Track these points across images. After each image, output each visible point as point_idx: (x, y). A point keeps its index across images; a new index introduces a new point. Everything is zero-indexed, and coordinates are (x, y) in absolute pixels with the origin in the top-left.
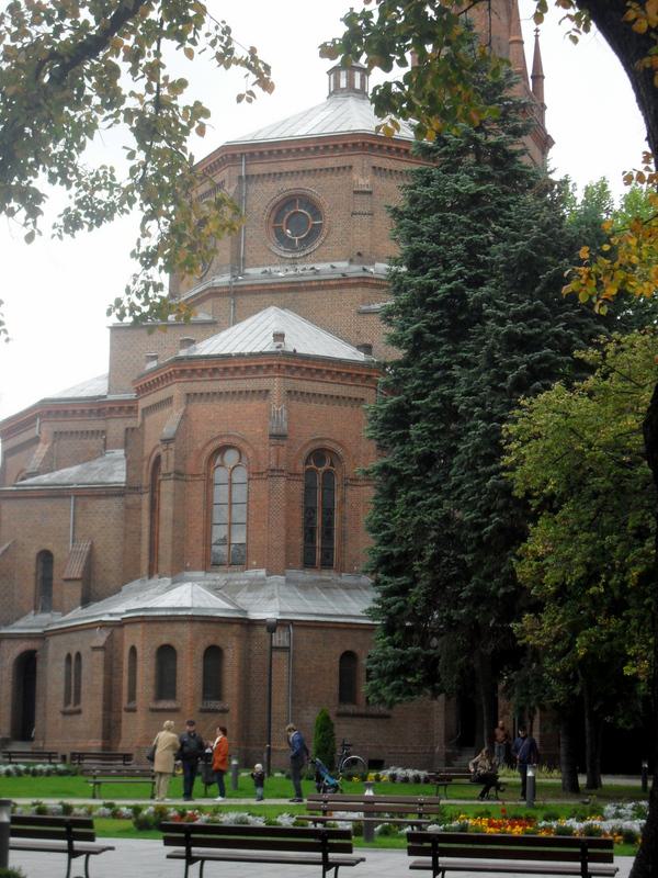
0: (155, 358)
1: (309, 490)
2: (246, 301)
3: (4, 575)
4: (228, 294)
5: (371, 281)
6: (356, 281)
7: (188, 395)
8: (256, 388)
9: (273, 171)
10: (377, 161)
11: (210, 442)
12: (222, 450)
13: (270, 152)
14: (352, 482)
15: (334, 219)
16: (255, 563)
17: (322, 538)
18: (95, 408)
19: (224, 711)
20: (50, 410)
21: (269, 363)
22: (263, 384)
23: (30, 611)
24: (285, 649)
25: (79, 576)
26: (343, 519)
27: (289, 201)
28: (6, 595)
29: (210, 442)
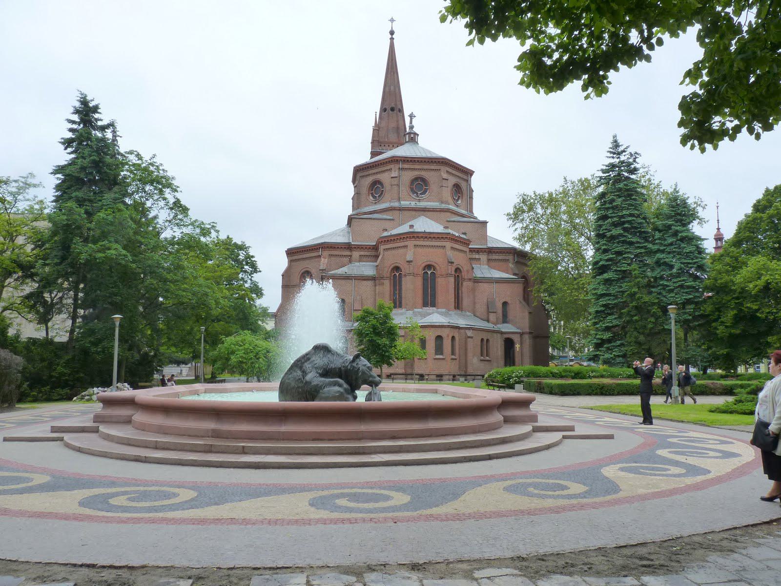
0: (386, 230)
2: (406, 213)
4: (400, 210)
8: (441, 245)
13: (411, 161)
15: (433, 187)
18: (348, 247)
19: (456, 359)
24: (472, 337)
27: (416, 179)
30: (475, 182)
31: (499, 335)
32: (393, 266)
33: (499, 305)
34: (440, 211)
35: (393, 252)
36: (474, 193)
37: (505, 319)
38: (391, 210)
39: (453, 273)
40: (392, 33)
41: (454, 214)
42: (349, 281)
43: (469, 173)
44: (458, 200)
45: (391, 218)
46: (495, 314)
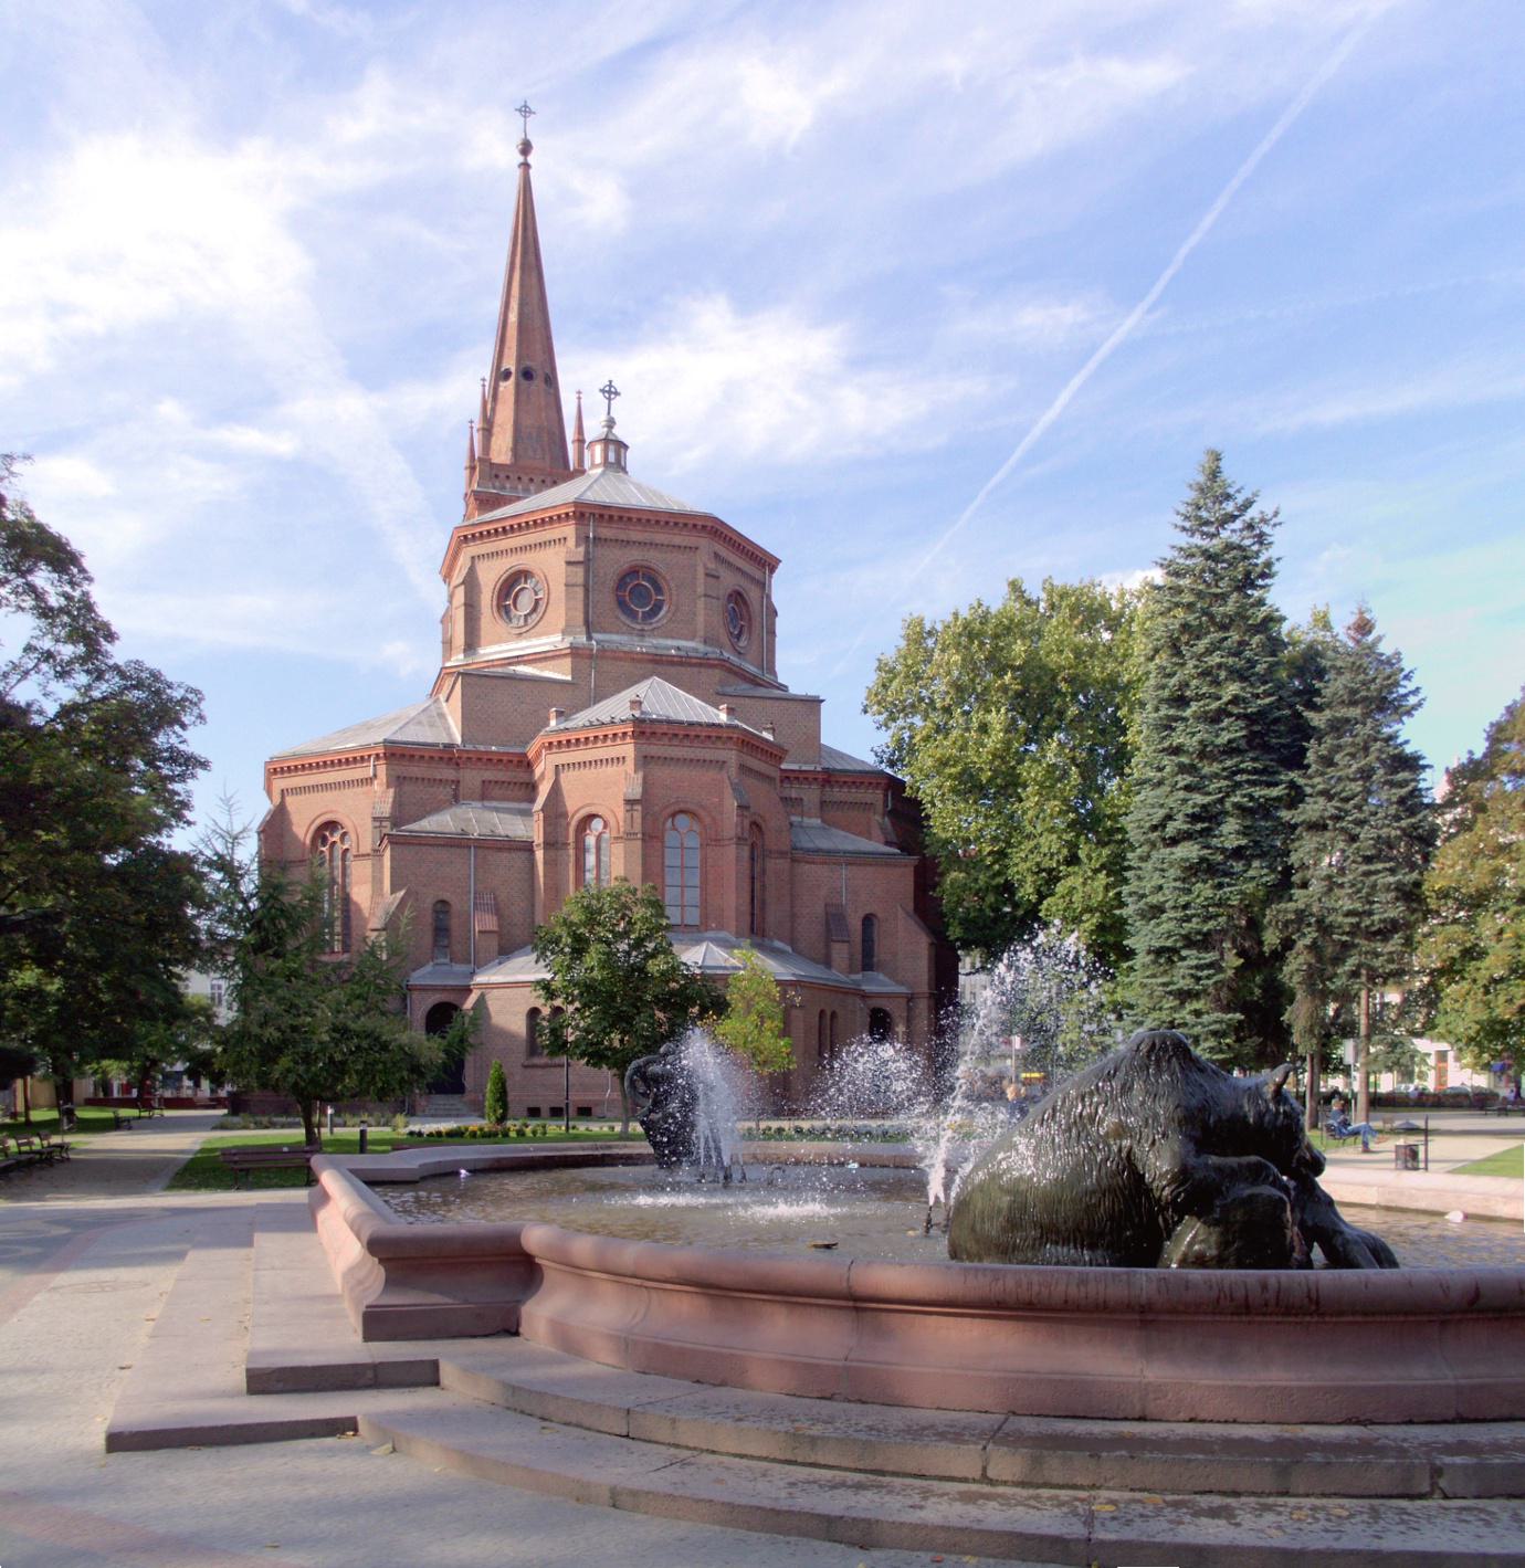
12: (674, 815)
18: (446, 755)
20: (396, 753)
25: (496, 929)
26: (763, 887)
27: (633, 572)
30: (781, 589)
31: (859, 1003)
33: (855, 924)
34: (701, 665)
35: (588, 774)
36: (777, 620)
37: (868, 962)
38: (565, 655)
39: (746, 835)
40: (526, 148)
41: (736, 674)
42: (458, 851)
43: (766, 563)
44: (738, 637)
45: (569, 678)
46: (845, 946)
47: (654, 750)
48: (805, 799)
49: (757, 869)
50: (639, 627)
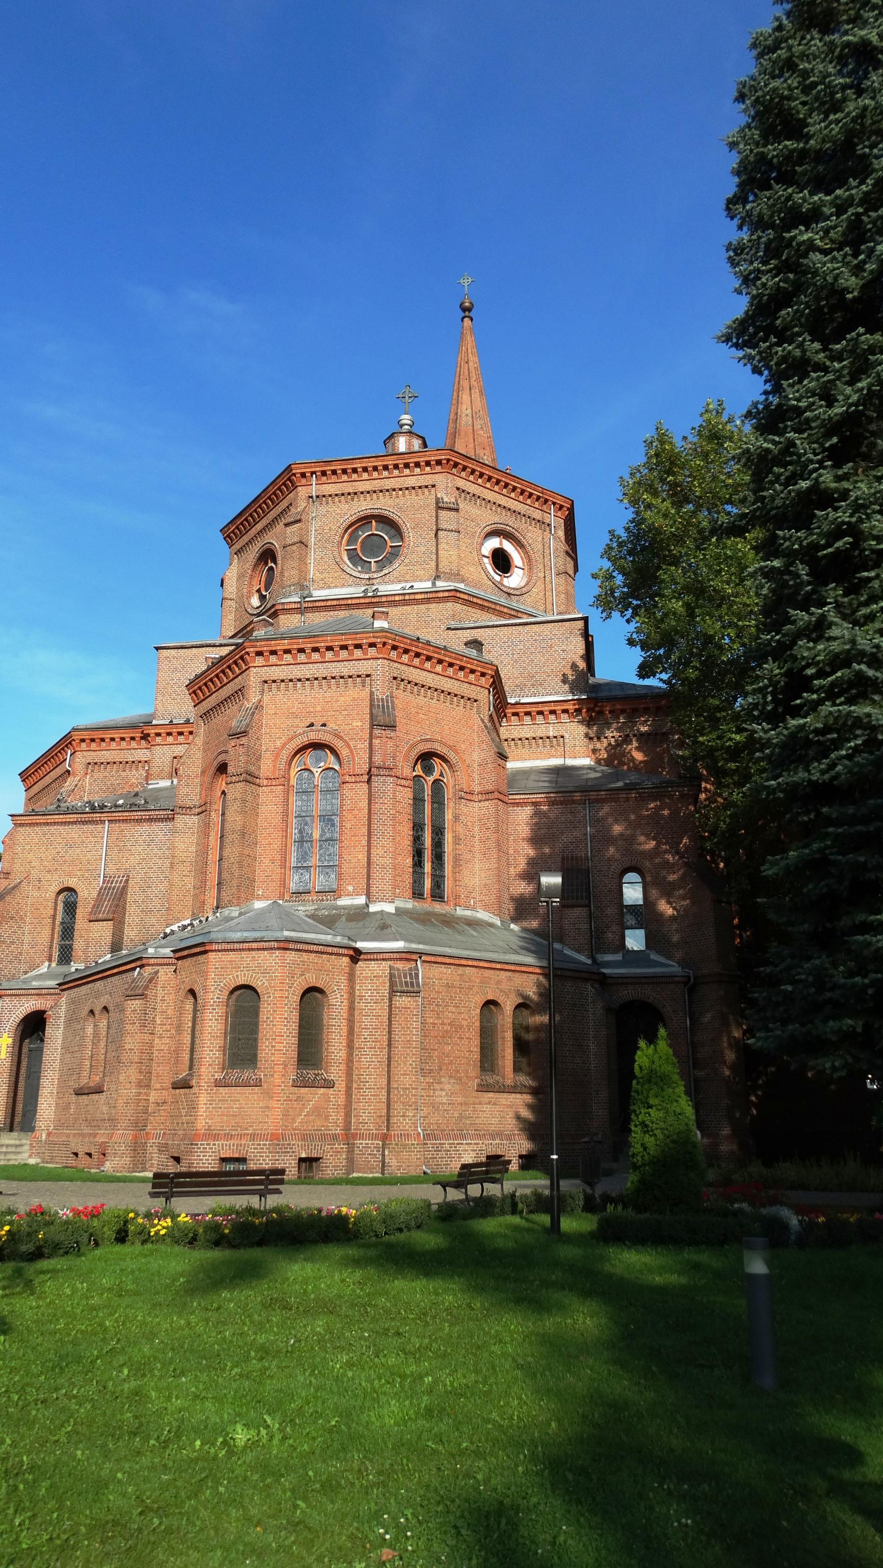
1: (418, 801)
3: (12, 918)
5: (462, 596)
6: (447, 594)
7: (266, 682)
9: (346, 491)
10: (461, 483)
11: (291, 739)
14: (466, 796)
16: (350, 888)
17: (433, 862)
21: (372, 640)
22: (364, 667)
23: (43, 962)
27: (365, 520)
28: (13, 943)
29: (291, 739)
31: (590, 989)
32: (215, 764)
41: (482, 607)
42: (91, 827)
47: (277, 673)
48: (567, 736)
49: (449, 816)
50: (367, 576)
